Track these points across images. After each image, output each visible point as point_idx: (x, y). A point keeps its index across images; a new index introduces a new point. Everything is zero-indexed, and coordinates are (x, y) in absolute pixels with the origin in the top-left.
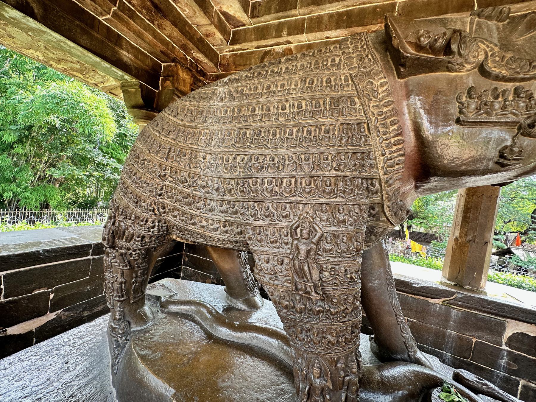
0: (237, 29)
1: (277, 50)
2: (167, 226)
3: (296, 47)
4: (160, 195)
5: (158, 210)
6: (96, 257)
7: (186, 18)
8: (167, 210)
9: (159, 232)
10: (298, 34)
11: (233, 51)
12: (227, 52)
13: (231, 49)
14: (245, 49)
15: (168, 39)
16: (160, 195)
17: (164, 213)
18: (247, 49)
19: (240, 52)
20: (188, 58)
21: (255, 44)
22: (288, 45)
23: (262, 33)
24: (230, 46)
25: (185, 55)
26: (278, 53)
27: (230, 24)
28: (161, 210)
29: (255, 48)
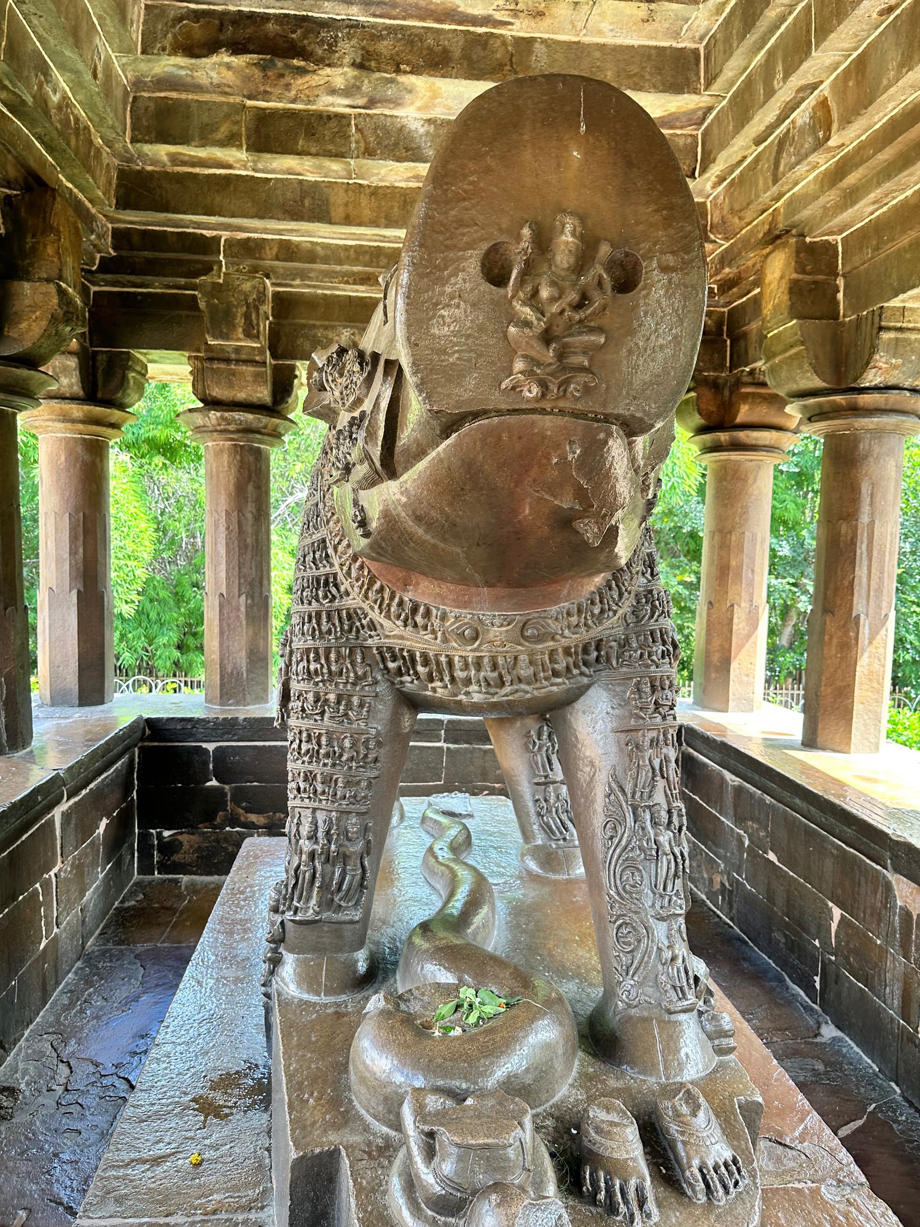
0: (706, 124)
1: (799, 122)
3: (834, 85)
6: (451, 746)
10: (801, 63)
11: (721, 179)
13: (713, 179)
18: (745, 158)
19: (737, 172)
22: (816, 92)
23: (743, 106)
24: (707, 175)
27: (681, 128)
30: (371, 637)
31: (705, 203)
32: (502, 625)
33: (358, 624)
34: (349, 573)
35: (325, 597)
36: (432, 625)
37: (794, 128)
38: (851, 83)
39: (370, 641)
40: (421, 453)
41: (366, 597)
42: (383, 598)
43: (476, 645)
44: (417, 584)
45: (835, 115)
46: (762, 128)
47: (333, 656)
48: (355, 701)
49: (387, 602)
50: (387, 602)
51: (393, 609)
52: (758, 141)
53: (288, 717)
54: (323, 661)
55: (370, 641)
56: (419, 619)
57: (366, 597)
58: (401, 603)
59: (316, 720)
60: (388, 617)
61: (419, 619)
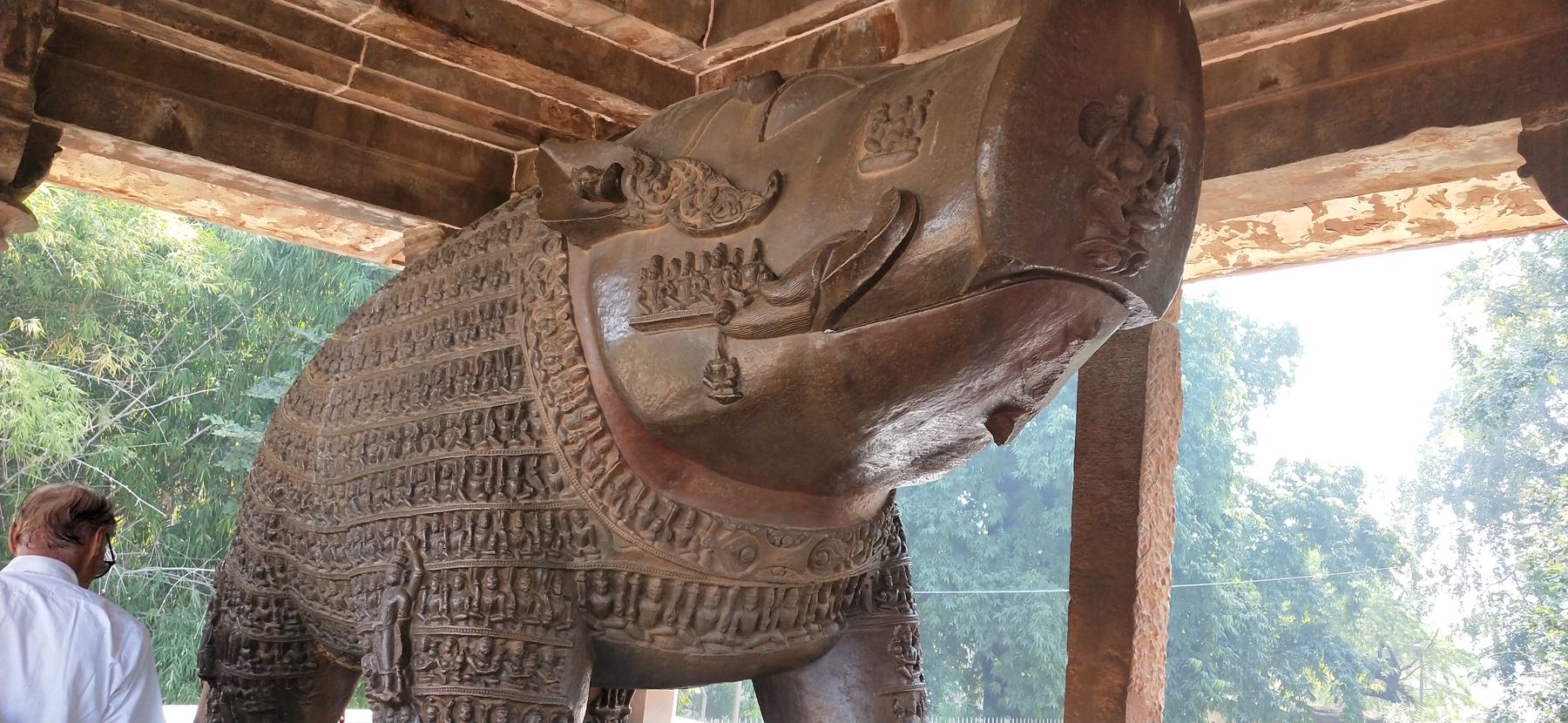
1: (852, 28)
2: (298, 617)
4: (273, 538)
5: (273, 574)
7: (555, 19)
8: (289, 575)
9: (282, 629)
11: (728, 57)
12: (712, 64)
13: (720, 54)
14: (762, 46)
15: (513, 85)
16: (273, 538)
17: (285, 580)
18: (768, 43)
19: (750, 55)
20: (592, 114)
21: (778, 26)
24: (712, 49)
25: (577, 112)
26: (855, 37)
28: (279, 575)
29: (789, 34)
30: (582, 554)
31: (693, 77)
32: (794, 545)
33: (564, 534)
34: (578, 457)
35: (520, 490)
36: (698, 540)
37: (843, 31)
38: (928, 9)
39: (578, 561)
40: (910, 305)
41: (601, 493)
42: (628, 497)
43: (749, 570)
44: (690, 478)
45: (904, 34)
46: (807, 20)
47: (523, 583)
48: (547, 654)
49: (632, 503)
50: (632, 503)
51: (641, 514)
52: (790, 33)
53: (412, 683)
54: (506, 588)
55: (578, 561)
56: (681, 532)
57: (601, 493)
58: (656, 506)
59: (487, 684)
60: (629, 525)
61: (681, 532)
